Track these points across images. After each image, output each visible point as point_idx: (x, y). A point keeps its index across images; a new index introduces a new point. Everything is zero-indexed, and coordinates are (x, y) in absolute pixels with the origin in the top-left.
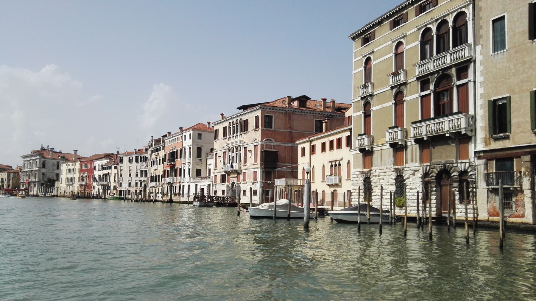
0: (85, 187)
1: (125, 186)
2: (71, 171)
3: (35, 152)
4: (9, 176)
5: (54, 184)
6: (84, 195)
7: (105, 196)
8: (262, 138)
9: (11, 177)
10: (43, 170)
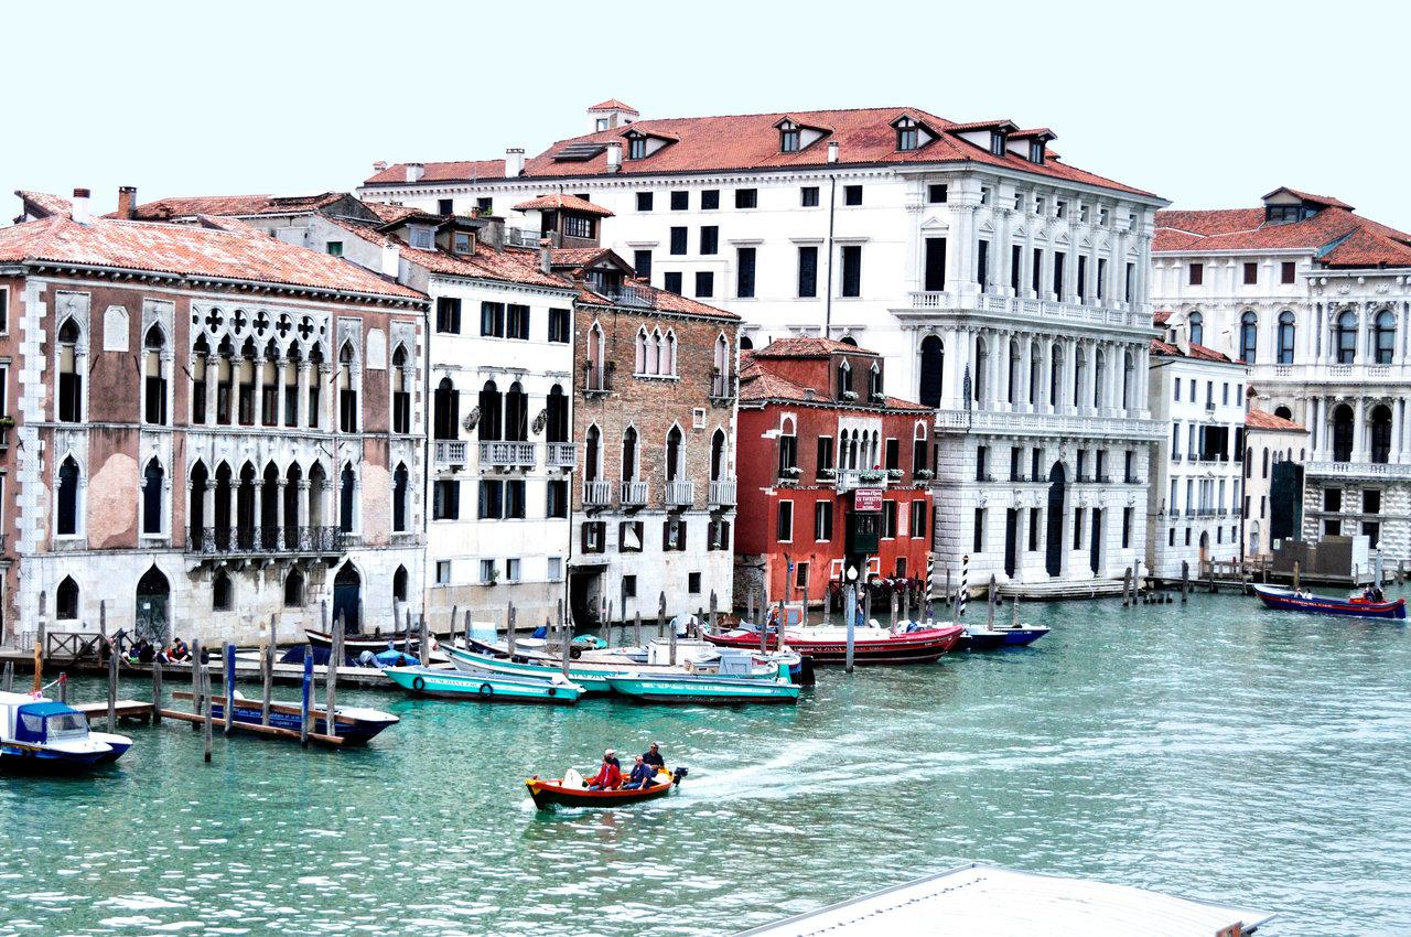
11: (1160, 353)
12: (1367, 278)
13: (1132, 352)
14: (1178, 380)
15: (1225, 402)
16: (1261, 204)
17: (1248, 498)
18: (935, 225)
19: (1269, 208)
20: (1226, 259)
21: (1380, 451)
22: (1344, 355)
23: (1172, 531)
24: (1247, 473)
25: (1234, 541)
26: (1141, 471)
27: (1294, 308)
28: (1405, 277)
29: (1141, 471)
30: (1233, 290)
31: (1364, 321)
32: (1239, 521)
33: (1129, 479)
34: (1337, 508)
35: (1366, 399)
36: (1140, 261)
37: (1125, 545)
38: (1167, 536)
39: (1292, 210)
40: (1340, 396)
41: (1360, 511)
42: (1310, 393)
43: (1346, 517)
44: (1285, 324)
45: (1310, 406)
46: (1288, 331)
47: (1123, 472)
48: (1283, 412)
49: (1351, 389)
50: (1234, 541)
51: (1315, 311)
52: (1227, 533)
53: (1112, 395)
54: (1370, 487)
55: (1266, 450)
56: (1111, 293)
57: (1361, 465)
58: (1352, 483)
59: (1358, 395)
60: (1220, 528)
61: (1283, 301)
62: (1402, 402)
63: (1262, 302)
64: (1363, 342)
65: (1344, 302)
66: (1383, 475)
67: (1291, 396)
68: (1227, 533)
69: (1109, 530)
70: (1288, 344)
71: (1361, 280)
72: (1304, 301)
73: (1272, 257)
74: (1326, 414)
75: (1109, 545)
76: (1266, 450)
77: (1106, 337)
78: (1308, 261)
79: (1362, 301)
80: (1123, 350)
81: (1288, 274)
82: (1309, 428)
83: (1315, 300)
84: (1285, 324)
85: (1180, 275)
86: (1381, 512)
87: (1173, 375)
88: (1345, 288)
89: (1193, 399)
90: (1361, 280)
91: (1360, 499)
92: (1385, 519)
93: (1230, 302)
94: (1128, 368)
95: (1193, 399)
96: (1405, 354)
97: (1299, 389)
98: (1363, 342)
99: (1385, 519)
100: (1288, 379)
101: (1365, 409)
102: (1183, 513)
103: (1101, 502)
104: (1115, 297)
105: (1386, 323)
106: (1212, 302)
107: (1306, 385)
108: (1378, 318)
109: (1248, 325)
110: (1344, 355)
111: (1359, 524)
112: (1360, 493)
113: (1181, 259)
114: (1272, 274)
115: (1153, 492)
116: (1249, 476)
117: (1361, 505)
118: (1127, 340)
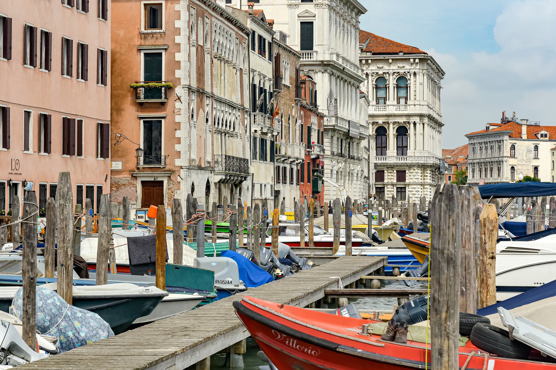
12: (392, 59)
18: (307, 15)
21: (402, 149)
28: (414, 59)
31: (392, 82)
35: (394, 123)
41: (395, 181)
58: (391, 167)
62: (415, 124)
65: (381, 72)
71: (390, 61)
79: (391, 72)
90: (390, 61)
91: (395, 175)
112: (395, 172)
117: (395, 178)
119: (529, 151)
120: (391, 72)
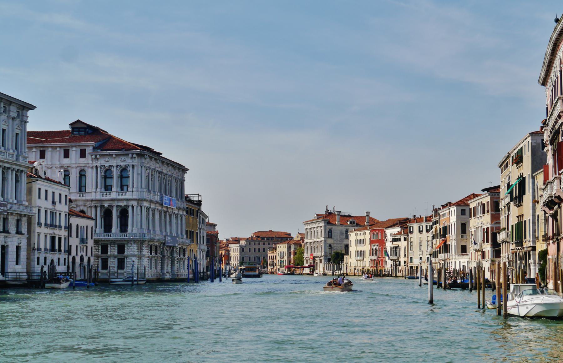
0: (377, 262)
1: (416, 262)
2: (361, 242)
3: (319, 216)
4: (289, 248)
5: (342, 260)
6: (376, 273)
7: (396, 273)
8: (492, 221)
9: (292, 250)
10: (330, 241)
11: (31, 176)
12: (116, 155)
13: (19, 174)
14: (40, 189)
15: (60, 202)
16: (69, 128)
17: (71, 246)
19: (73, 129)
20: (56, 148)
21: (124, 227)
22: (108, 188)
23: (38, 258)
24: (70, 235)
25: (65, 265)
26: (24, 230)
27: (86, 169)
28: (132, 154)
29: (24, 230)
30: (59, 161)
31: (115, 173)
32: (67, 256)
33: (19, 232)
34: (107, 253)
35: (117, 206)
36: (21, 132)
37: (17, 263)
38: (36, 260)
39: (82, 131)
40: (106, 205)
41: (116, 253)
42: (93, 204)
43: (110, 256)
44: (82, 175)
45: (94, 210)
46: (83, 178)
47: (15, 229)
48: (83, 212)
49: (111, 202)
50: (65, 265)
51: (94, 169)
52: (62, 261)
53: (10, 189)
54: (120, 243)
55: (77, 225)
56: (8, 145)
57: (116, 234)
58: (113, 242)
59: (114, 204)
60: (59, 259)
61: (81, 165)
62: (133, 207)
63: (71, 166)
64: (115, 182)
66: (126, 237)
67: (85, 206)
68: (62, 261)
69: (10, 256)
70: (83, 184)
71: (114, 156)
72: (90, 165)
73: (75, 146)
74: (101, 213)
75: (9, 263)
76: (77, 225)
77: (7, 165)
78: (91, 148)
79: (115, 164)
80: (14, 172)
81: (83, 154)
82: (93, 216)
83: (95, 165)
84: (82, 175)
85: (36, 155)
86: (125, 253)
87: (38, 186)
88: (107, 159)
89: (46, 199)
90: (114, 156)
91: (116, 248)
92: (127, 257)
93: (58, 166)
94: (17, 181)
95: (46, 199)
96: (133, 187)
97: (89, 203)
98: (115, 182)
99: (127, 257)
100: (84, 198)
101: (117, 211)
102: (43, 250)
103: (5, 242)
104: (10, 147)
105: (124, 175)
106: (49, 166)
107: (92, 200)
108: (121, 172)
109: (67, 175)
110: (108, 188)
111: (116, 259)
113: (36, 147)
114: (76, 153)
115: (29, 239)
116: (71, 236)
117: (116, 251)
118: (17, 168)
119: (342, 234)
120: (115, 164)
